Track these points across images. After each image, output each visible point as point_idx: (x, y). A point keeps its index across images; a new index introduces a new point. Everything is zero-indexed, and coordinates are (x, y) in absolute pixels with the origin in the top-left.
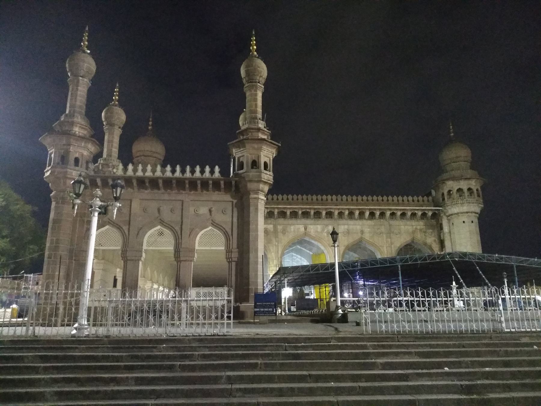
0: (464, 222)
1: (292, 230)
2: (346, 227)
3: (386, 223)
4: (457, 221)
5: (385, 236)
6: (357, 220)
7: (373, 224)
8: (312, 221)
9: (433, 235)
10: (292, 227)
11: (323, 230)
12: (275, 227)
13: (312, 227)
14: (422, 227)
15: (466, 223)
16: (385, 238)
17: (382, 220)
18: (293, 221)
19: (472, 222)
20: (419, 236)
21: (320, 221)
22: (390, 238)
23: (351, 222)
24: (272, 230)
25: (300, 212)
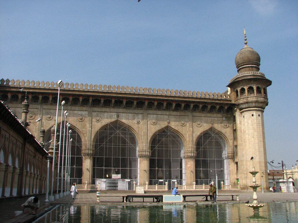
0: (253, 115)
3: (189, 114)
4: (247, 114)
6: (164, 110)
7: (179, 114)
8: (124, 110)
13: (124, 115)
15: (255, 116)
16: (188, 127)
17: (186, 111)
18: (108, 109)
19: (259, 115)
21: (131, 111)
23: (159, 112)
25: (113, 101)
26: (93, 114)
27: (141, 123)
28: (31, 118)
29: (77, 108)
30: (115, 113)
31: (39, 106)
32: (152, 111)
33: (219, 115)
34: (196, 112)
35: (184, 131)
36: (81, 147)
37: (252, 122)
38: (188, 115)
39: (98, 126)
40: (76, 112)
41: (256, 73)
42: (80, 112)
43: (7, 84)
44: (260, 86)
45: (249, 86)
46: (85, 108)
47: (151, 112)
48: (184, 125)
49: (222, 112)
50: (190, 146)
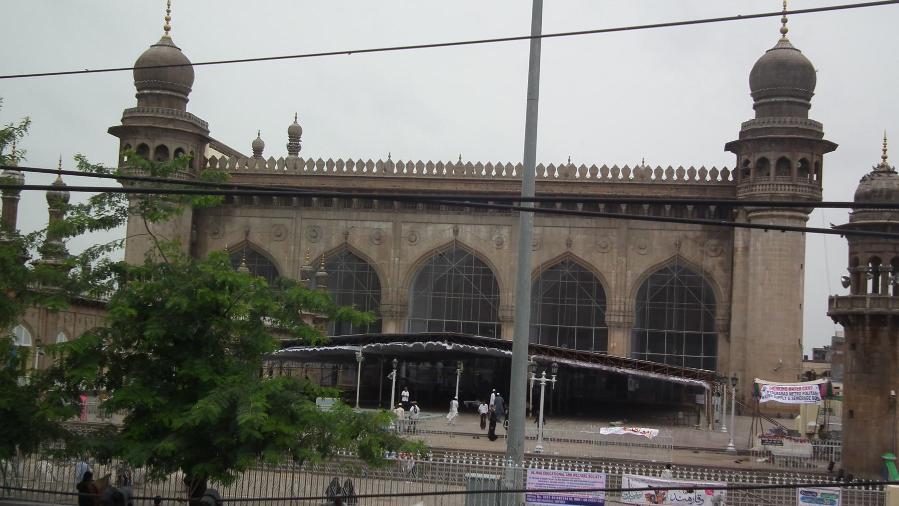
1: (430, 233)
5: (616, 250)
7: (594, 225)
8: (470, 218)
9: (719, 252)
10: (430, 228)
11: (491, 237)
13: (469, 228)
14: (698, 234)
18: (433, 217)
20: (689, 253)
21: (485, 220)
22: (626, 255)
24: (390, 232)
27: (506, 247)
28: (280, 239)
30: (450, 226)
31: (292, 213)
36: (379, 298)
37: (762, 245)
39: (414, 253)
40: (367, 224)
42: (376, 225)
44: (787, 155)
45: (758, 156)
46: (385, 216)
50: (617, 299)
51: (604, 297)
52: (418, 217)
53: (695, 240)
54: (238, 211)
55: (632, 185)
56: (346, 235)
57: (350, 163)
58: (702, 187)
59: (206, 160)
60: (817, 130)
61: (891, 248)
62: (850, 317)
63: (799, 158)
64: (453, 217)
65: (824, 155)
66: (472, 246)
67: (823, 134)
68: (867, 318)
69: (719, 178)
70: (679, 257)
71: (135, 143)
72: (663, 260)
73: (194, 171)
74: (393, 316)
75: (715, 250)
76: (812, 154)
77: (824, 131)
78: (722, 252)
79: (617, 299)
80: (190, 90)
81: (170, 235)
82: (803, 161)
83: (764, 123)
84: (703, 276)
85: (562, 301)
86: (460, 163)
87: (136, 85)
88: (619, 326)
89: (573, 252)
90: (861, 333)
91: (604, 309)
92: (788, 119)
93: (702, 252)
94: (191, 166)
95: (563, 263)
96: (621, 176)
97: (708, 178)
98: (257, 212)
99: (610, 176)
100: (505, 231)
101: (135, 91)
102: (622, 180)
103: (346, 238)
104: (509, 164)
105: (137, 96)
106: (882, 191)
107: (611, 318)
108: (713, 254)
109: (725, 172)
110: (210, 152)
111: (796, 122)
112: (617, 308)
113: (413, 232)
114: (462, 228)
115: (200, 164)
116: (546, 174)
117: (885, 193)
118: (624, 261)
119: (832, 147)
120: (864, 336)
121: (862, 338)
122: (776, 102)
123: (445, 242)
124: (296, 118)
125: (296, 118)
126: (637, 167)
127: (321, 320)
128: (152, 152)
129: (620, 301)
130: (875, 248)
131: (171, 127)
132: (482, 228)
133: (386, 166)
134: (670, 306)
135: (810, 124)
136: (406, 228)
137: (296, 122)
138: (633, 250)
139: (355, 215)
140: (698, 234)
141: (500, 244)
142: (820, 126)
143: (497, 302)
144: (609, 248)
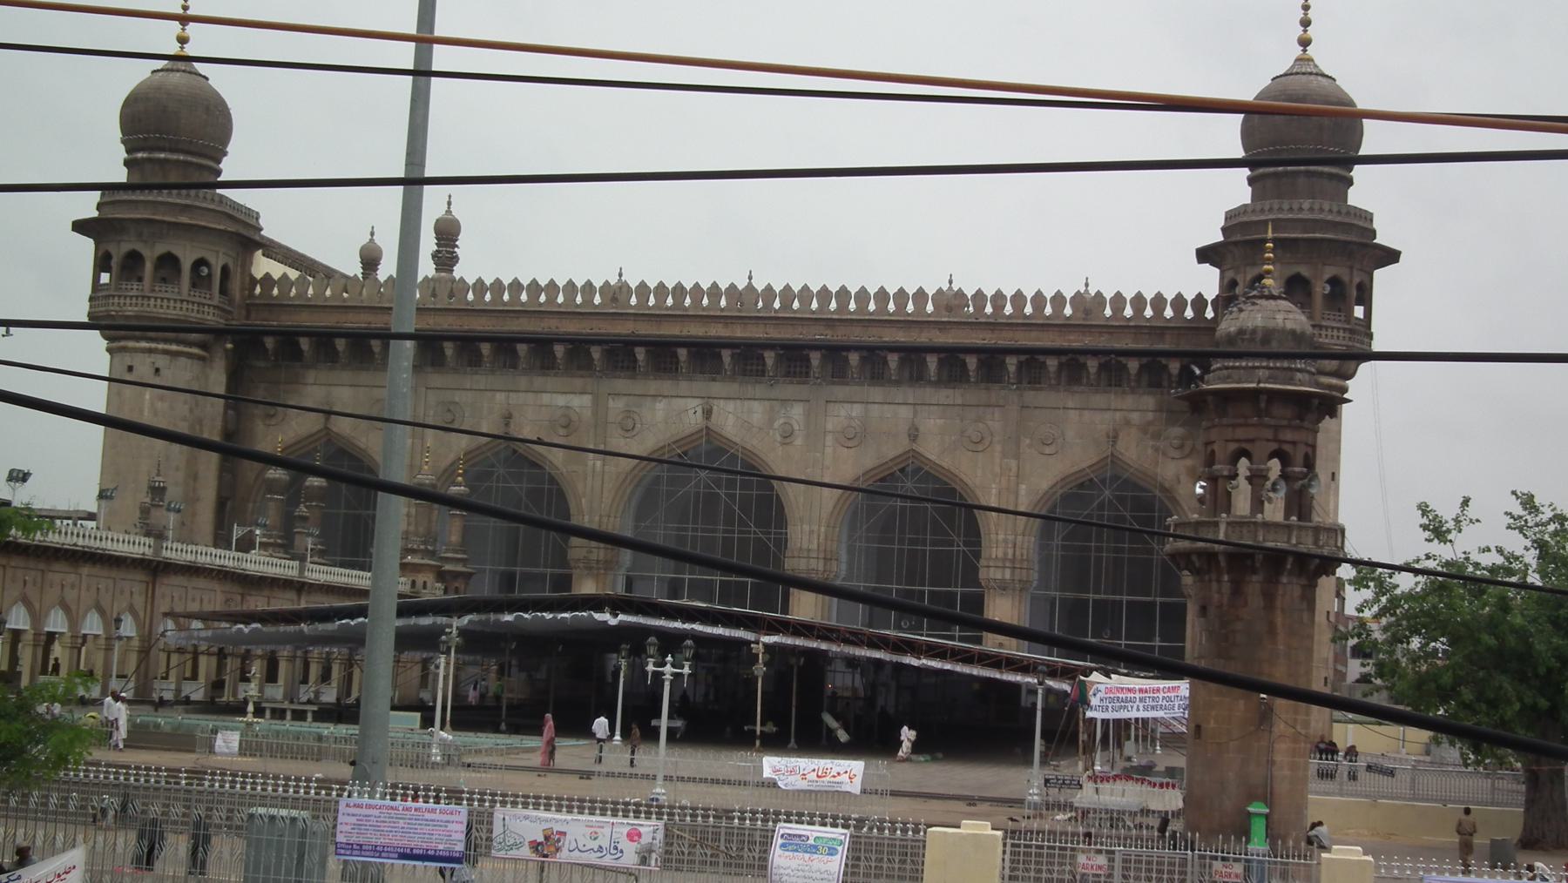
1: (660, 415)
2: (857, 410)
5: (998, 448)
6: (898, 383)
8: (734, 388)
9: (1187, 450)
10: (661, 405)
11: (771, 421)
12: (596, 403)
13: (731, 406)
14: (1150, 416)
17: (997, 386)
18: (666, 386)
20: (1134, 452)
21: (760, 390)
22: (1017, 457)
23: (876, 393)
24: (588, 413)
26: (611, 403)
27: (799, 442)
29: (550, 382)
30: (697, 402)
32: (847, 389)
33: (1149, 401)
34: (1041, 389)
35: (979, 473)
38: (1001, 402)
40: (546, 398)
41: (1291, 209)
42: (561, 400)
43: (298, 295)
44: (1304, 271)
47: (841, 391)
48: (980, 448)
49: (1165, 383)
50: (1001, 537)
51: (978, 535)
52: (638, 386)
53: (1144, 429)
54: (311, 376)
55: (1066, 327)
56: (508, 418)
57: (516, 286)
58: (1157, 329)
59: (254, 281)
60: (1361, 223)
61: (1269, 434)
62: (1194, 558)
63: (1327, 276)
64: (701, 386)
65: (1376, 273)
66: (737, 440)
67: (1374, 232)
68: (1222, 559)
69: (1189, 313)
70: (1114, 459)
71: (119, 250)
72: (1084, 465)
73: (231, 302)
74: (591, 568)
75: (1181, 447)
76: (1351, 268)
77: (1375, 226)
78: (1193, 449)
79: (1001, 537)
80: (225, 154)
81: (184, 419)
82: (1334, 281)
83: (1262, 211)
84: (1157, 493)
85: (901, 542)
86: (750, 287)
87: (123, 142)
88: (1003, 587)
89: (920, 450)
90: (1214, 586)
91: (978, 555)
92: (1306, 205)
93: (1156, 450)
94: (224, 291)
95: (902, 470)
96: (1008, 310)
97: (1169, 313)
98: (346, 376)
99: (989, 309)
100: (797, 411)
101: (122, 153)
102: (1010, 316)
103: (507, 425)
104: (715, 286)
105: (127, 163)
106: (1254, 331)
107: (990, 572)
108: (1176, 454)
109: (1199, 302)
110: (263, 266)
111: (1321, 210)
112: (1000, 555)
113: (628, 413)
114: (719, 406)
115: (242, 289)
116: (872, 307)
117: (1259, 336)
118: (1014, 469)
119: (1391, 256)
120: (1219, 592)
121: (1216, 596)
122: (1286, 174)
123: (687, 432)
124: (449, 203)
125: (449, 203)
126: (940, 291)
127: (456, 575)
128: (149, 266)
129: (1005, 541)
130: (1241, 433)
131: (184, 219)
132: (756, 405)
133: (615, 293)
134: (1099, 549)
135: (1348, 213)
136: (616, 406)
137: (449, 212)
138: (1030, 446)
139: (523, 381)
140: (1150, 416)
141: (788, 436)
142: (1368, 217)
143: (781, 543)
144: (987, 442)
